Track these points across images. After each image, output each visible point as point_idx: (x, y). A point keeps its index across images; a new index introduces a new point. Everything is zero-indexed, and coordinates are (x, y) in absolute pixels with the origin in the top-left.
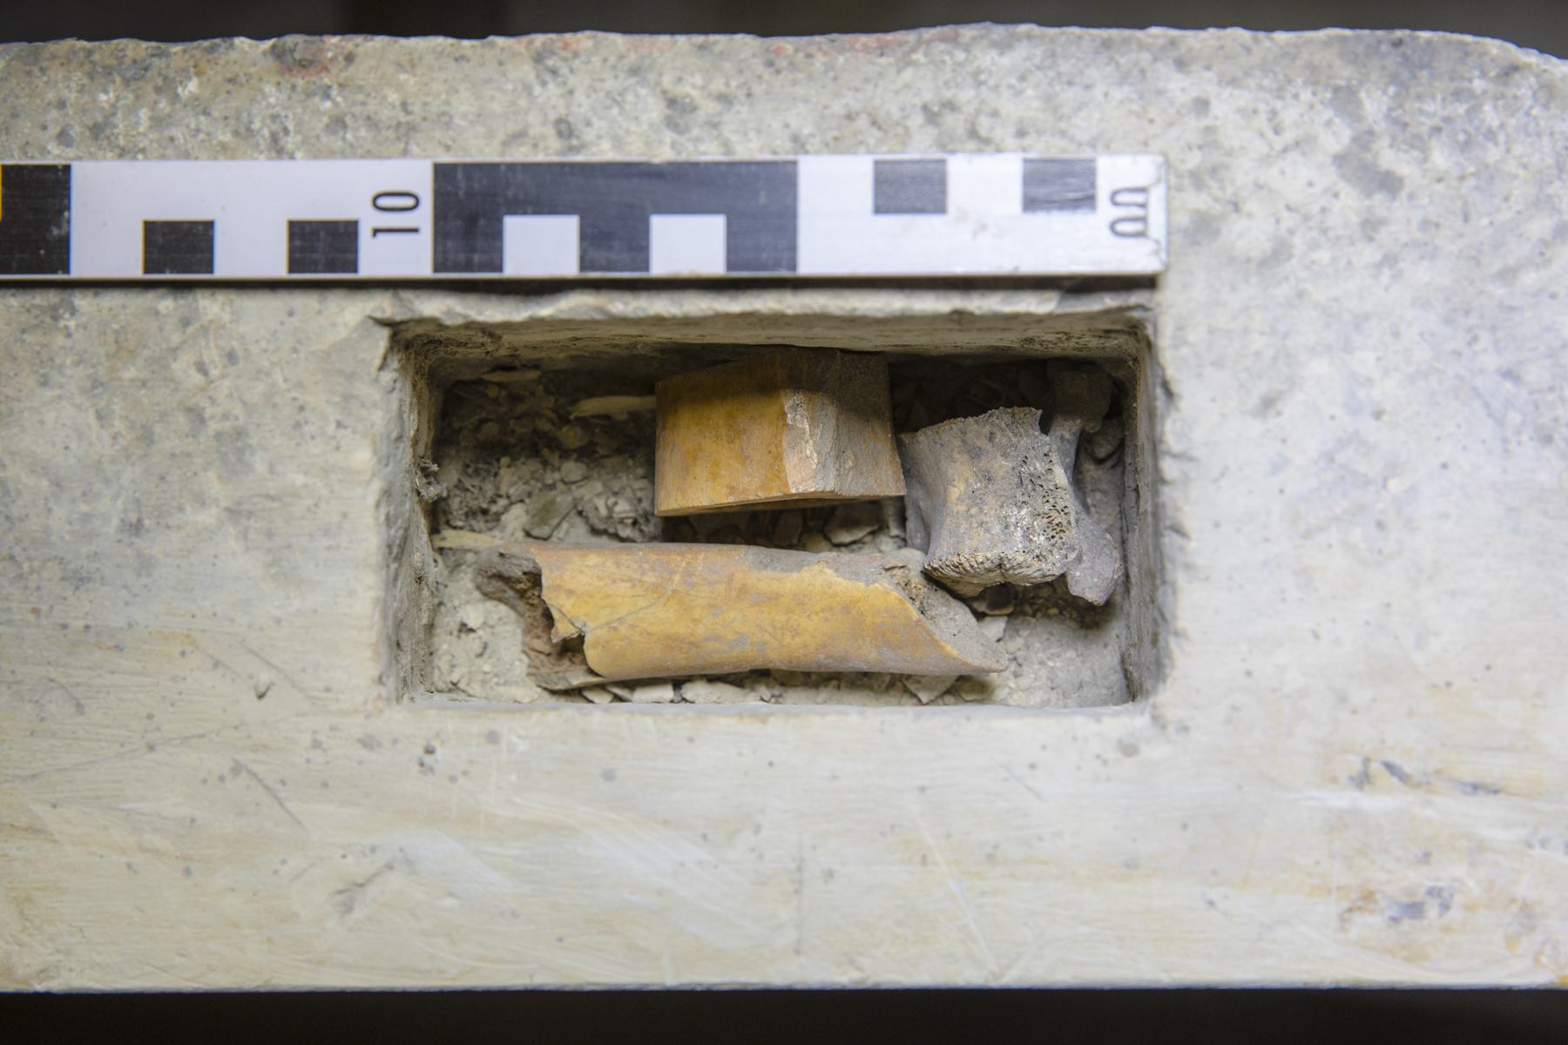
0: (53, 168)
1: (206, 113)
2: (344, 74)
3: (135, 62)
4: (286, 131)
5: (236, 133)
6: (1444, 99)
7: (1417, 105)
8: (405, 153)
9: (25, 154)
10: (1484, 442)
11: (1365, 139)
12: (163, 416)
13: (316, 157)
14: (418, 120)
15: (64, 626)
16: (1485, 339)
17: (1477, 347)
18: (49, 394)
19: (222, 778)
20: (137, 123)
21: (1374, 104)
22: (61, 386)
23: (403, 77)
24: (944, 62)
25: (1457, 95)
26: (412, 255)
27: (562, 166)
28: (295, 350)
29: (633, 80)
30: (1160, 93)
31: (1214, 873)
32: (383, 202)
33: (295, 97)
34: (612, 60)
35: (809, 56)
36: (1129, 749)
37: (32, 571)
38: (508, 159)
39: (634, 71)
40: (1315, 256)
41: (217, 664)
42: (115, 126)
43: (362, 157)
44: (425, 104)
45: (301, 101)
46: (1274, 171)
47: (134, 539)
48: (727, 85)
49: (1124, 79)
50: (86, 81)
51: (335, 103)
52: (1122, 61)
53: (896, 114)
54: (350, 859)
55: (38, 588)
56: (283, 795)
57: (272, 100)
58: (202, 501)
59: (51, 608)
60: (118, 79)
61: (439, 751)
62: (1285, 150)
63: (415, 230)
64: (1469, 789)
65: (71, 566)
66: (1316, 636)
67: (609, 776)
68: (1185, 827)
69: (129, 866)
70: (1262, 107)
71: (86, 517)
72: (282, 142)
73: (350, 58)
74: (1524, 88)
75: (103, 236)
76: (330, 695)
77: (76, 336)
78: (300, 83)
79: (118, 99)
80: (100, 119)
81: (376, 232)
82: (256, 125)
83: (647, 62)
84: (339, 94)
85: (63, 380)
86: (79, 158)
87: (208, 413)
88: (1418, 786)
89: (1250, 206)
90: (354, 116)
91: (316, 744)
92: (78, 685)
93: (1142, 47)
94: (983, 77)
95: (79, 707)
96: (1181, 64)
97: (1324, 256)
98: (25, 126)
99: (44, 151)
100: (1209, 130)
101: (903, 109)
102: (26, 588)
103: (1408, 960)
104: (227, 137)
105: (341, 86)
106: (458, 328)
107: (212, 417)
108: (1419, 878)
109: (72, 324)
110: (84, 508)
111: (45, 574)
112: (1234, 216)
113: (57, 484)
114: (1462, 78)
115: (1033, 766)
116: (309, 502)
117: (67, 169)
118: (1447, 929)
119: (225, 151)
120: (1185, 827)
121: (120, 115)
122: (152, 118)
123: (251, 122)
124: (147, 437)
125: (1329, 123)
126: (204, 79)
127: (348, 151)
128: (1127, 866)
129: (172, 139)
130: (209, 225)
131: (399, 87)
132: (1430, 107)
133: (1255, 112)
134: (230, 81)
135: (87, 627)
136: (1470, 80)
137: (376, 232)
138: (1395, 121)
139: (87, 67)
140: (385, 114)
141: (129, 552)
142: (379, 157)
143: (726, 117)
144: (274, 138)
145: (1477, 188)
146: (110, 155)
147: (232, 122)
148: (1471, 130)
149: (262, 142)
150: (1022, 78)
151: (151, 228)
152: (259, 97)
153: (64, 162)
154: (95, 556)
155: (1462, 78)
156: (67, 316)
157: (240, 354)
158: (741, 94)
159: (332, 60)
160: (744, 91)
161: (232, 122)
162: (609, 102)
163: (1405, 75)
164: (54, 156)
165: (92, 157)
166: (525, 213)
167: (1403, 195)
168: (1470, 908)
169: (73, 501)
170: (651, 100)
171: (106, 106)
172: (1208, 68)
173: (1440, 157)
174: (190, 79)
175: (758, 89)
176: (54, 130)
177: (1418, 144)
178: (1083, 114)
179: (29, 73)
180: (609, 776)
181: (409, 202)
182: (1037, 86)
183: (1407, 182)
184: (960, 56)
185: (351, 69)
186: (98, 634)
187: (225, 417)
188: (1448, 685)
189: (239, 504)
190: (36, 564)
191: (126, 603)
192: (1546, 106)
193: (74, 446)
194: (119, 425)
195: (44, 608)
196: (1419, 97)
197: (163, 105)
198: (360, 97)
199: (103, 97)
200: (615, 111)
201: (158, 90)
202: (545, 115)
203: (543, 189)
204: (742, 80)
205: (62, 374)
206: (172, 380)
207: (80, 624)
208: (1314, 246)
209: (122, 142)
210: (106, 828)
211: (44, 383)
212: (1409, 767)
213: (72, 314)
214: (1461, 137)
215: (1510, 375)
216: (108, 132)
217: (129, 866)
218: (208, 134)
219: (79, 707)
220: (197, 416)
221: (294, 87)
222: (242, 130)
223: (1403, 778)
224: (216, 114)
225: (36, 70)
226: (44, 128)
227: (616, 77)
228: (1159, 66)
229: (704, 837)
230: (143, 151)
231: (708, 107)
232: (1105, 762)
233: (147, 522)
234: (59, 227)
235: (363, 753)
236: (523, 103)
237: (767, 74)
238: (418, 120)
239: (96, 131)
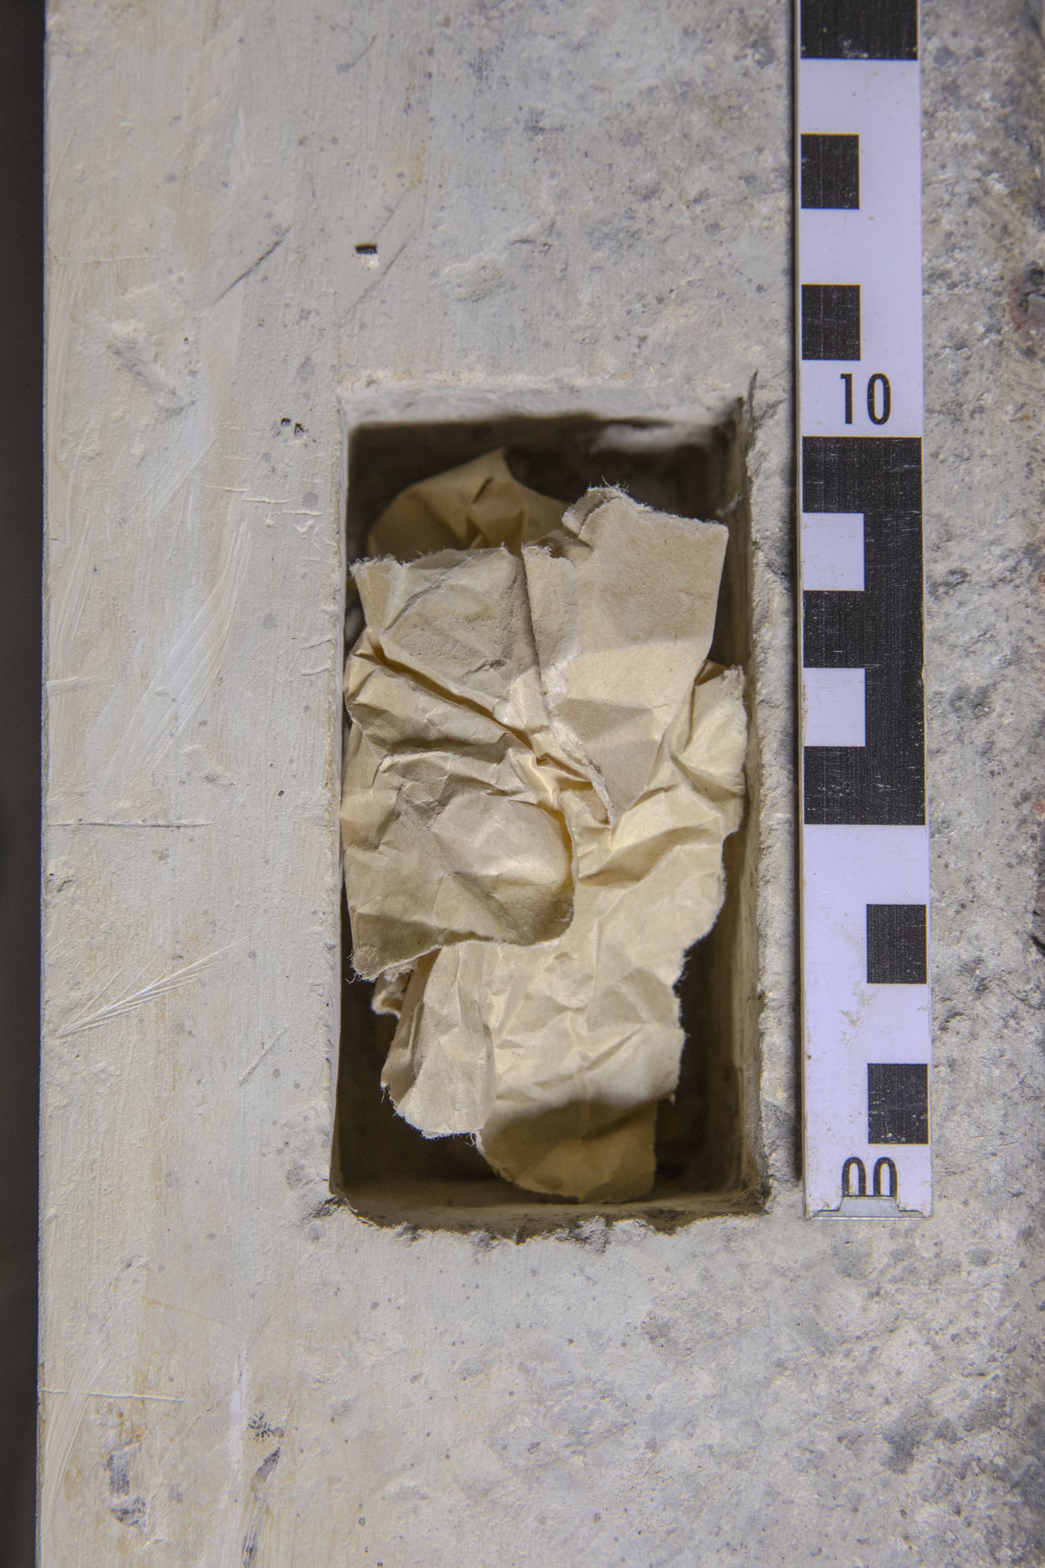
0: (914, 43)
1: (973, 201)
2: (1013, 348)
3: (1025, 128)
4: (952, 286)
5: (949, 235)
6: (990, 1517)
7: (984, 1488)
8: (930, 411)
9: (927, 15)
10: (623, 1560)
11: (946, 1434)
12: (653, 156)
13: (925, 317)
14: (965, 425)
15: (430, 52)
17: (725, 1554)
18: (675, 38)
19: (270, 215)
20: (960, 131)
21: (988, 1445)
22: (683, 50)
23: (1010, 408)
24: (1028, 981)
26: (823, 416)
27: (920, 576)
28: (721, 295)
29: (1007, 651)
30: (996, 1211)
31: (161, 1268)
32: (879, 385)
33: (989, 296)
34: (1029, 631)
35: (1034, 838)
36: (295, 1176)
37: (489, 19)
38: (925, 519)
39: (1016, 650)
40: (823, 1378)
41: (391, 211)
42: (957, 108)
43: (925, 366)
44: (981, 433)
45: (983, 301)
46: (913, 1335)
47: (522, 125)
48: (1004, 750)
49: (1011, 1174)
50: (1005, 78)
51: (984, 336)
52: (1029, 1172)
53: (973, 930)
54: (185, 348)
55: (471, 25)
56: (252, 278)
57: (985, 271)
58: (561, 196)
59: (451, 39)
60: (1007, 110)
61: (297, 442)
62: (935, 1347)
63: (849, 420)
64: (249, 1543)
65: (493, 59)
66: (415, 1378)
67: (269, 621)
68: (211, 1236)
69: (178, 118)
70: (982, 1321)
71: (546, 76)
72: (940, 282)
75: (841, 93)
76: (356, 330)
77: (737, 65)
78: (1004, 300)
79: (986, 110)
80: (964, 92)
81: (847, 378)
82: (958, 255)
83: (1027, 666)
84: (992, 341)
85: (690, 53)
86: (923, 71)
87: (655, 202)
88: (253, 1488)
89: (875, 1308)
90: (968, 358)
91: (305, 314)
92: (370, 66)
94: (1012, 1022)
95: (346, 67)
96: (1027, 1234)
97: (822, 1388)
98: (956, 16)
99: (929, 35)
100: (957, 1267)
101: (977, 937)
102: (471, 12)
103: (67, 1475)
104: (946, 225)
105: (1001, 343)
106: (745, 468)
107: (650, 207)
108: (153, 1486)
109: (749, 62)
110: (555, 74)
111: (486, 32)
112: (865, 1291)
114: (1013, 1538)
115: (277, 1073)
116: (561, 307)
117: (913, 56)
119: (931, 223)
120: (211, 1236)
121: (968, 112)
122: (965, 147)
123: (961, 249)
124: (630, 139)
125: (964, 1395)
126: (1007, 201)
127: (932, 351)
128: (169, 1175)
129: (943, 167)
130: (854, 204)
131: (999, 404)
132: (982, 1503)
133: (976, 1314)
134: (1005, 229)
135: (430, 76)
136: (1011, 1547)
137: (847, 378)
138: (966, 1465)
139: (1019, 79)
140: (969, 390)
141: (509, 119)
142: (926, 384)
143: (969, 752)
144: (943, 275)
145: (894, 1555)
146: (927, 102)
147: (963, 229)
148: (957, 1547)
149: (941, 261)
150: (1011, 1065)
151: (850, 143)
152: (987, 258)
153: (919, 53)
154: (504, 82)
155: (1013, 1538)
156: (757, 57)
157: (718, 237)
158: (994, 766)
159: (1028, 333)
160: (996, 769)
161: (963, 229)
162: (983, 626)
163: (1016, 1475)
164: (927, 45)
165: (925, 83)
166: (866, 535)
167: (889, 1474)
168: (122, 1544)
169: (562, 63)
170: (986, 669)
171: (978, 99)
172: (1022, 1265)
173: (928, 1515)
174: (1007, 186)
175: (998, 783)
176: (953, 44)
177: (943, 1491)
178: (973, 1131)
179: (1012, 18)
180: (269, 621)
181: (879, 414)
182: (1003, 1080)
183: (902, 1477)
185: (1017, 354)
186: (422, 87)
187: (651, 220)
188: (362, 1521)
189: (559, 234)
190: (496, 23)
191: (454, 117)
193: (620, 63)
194: (642, 110)
195: (449, 31)
196: (993, 1491)
197: (981, 158)
198: (988, 364)
199: (987, 95)
200: (975, 633)
201: (995, 153)
202: (970, 559)
203: (896, 551)
204: (1008, 767)
205: (696, 52)
206: (690, 165)
207: (433, 69)
208: (834, 1374)
209: (940, 114)
210: (218, 94)
211: (687, 32)
212: (275, 1476)
213: (759, 62)
214: (950, 1536)
216: (951, 100)
217: (178, 118)
218: (948, 205)
219: (346, 67)
220: (650, 194)
221: (999, 294)
222: (953, 240)
223: (262, 1473)
224: (970, 213)
225: (1016, 25)
226: (955, 34)
227: (1011, 634)
228: (1026, 1211)
229: (205, 723)
230: (931, 136)
231: (978, 734)
232: (280, 1151)
233: (540, 138)
234: (852, 48)
235: (296, 361)
236: (984, 535)
237: (1014, 793)
238: (965, 425)
239: (951, 89)
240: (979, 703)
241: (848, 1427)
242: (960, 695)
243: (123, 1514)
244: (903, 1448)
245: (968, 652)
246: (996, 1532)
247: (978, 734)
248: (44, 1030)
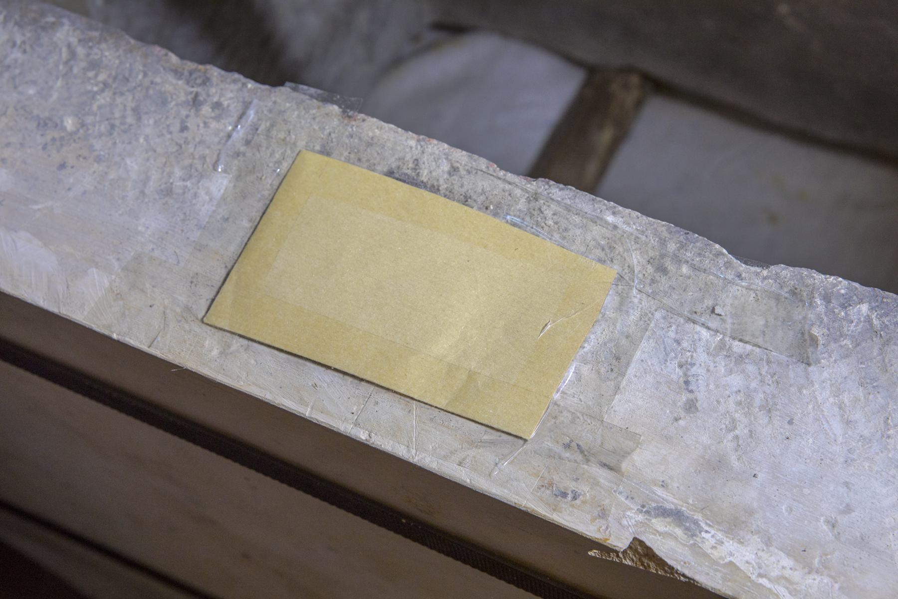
11: (663, 256)
16: (674, 327)
25: (700, 254)
73: (364, 120)
74: (721, 261)
93: (604, 204)
104: (316, 127)
108: (572, 485)
113: (211, 200)
118: (572, 506)
168: (584, 502)
173: (685, 269)
184: (547, 187)
192: (727, 268)
215: (678, 342)
240: (454, 170)
241: (648, 281)
242: (449, 173)
243: (575, 498)
244: (663, 270)
245: (439, 167)
246: (700, 254)
247: (463, 172)
248: (411, 461)
